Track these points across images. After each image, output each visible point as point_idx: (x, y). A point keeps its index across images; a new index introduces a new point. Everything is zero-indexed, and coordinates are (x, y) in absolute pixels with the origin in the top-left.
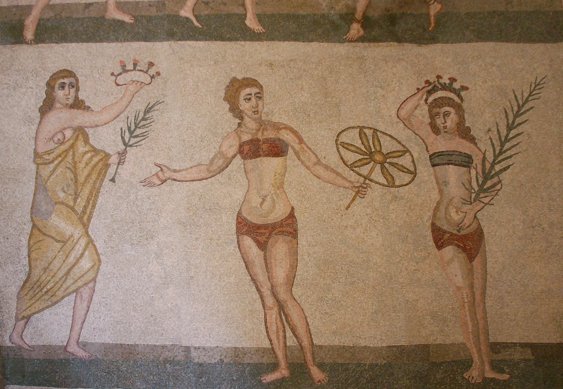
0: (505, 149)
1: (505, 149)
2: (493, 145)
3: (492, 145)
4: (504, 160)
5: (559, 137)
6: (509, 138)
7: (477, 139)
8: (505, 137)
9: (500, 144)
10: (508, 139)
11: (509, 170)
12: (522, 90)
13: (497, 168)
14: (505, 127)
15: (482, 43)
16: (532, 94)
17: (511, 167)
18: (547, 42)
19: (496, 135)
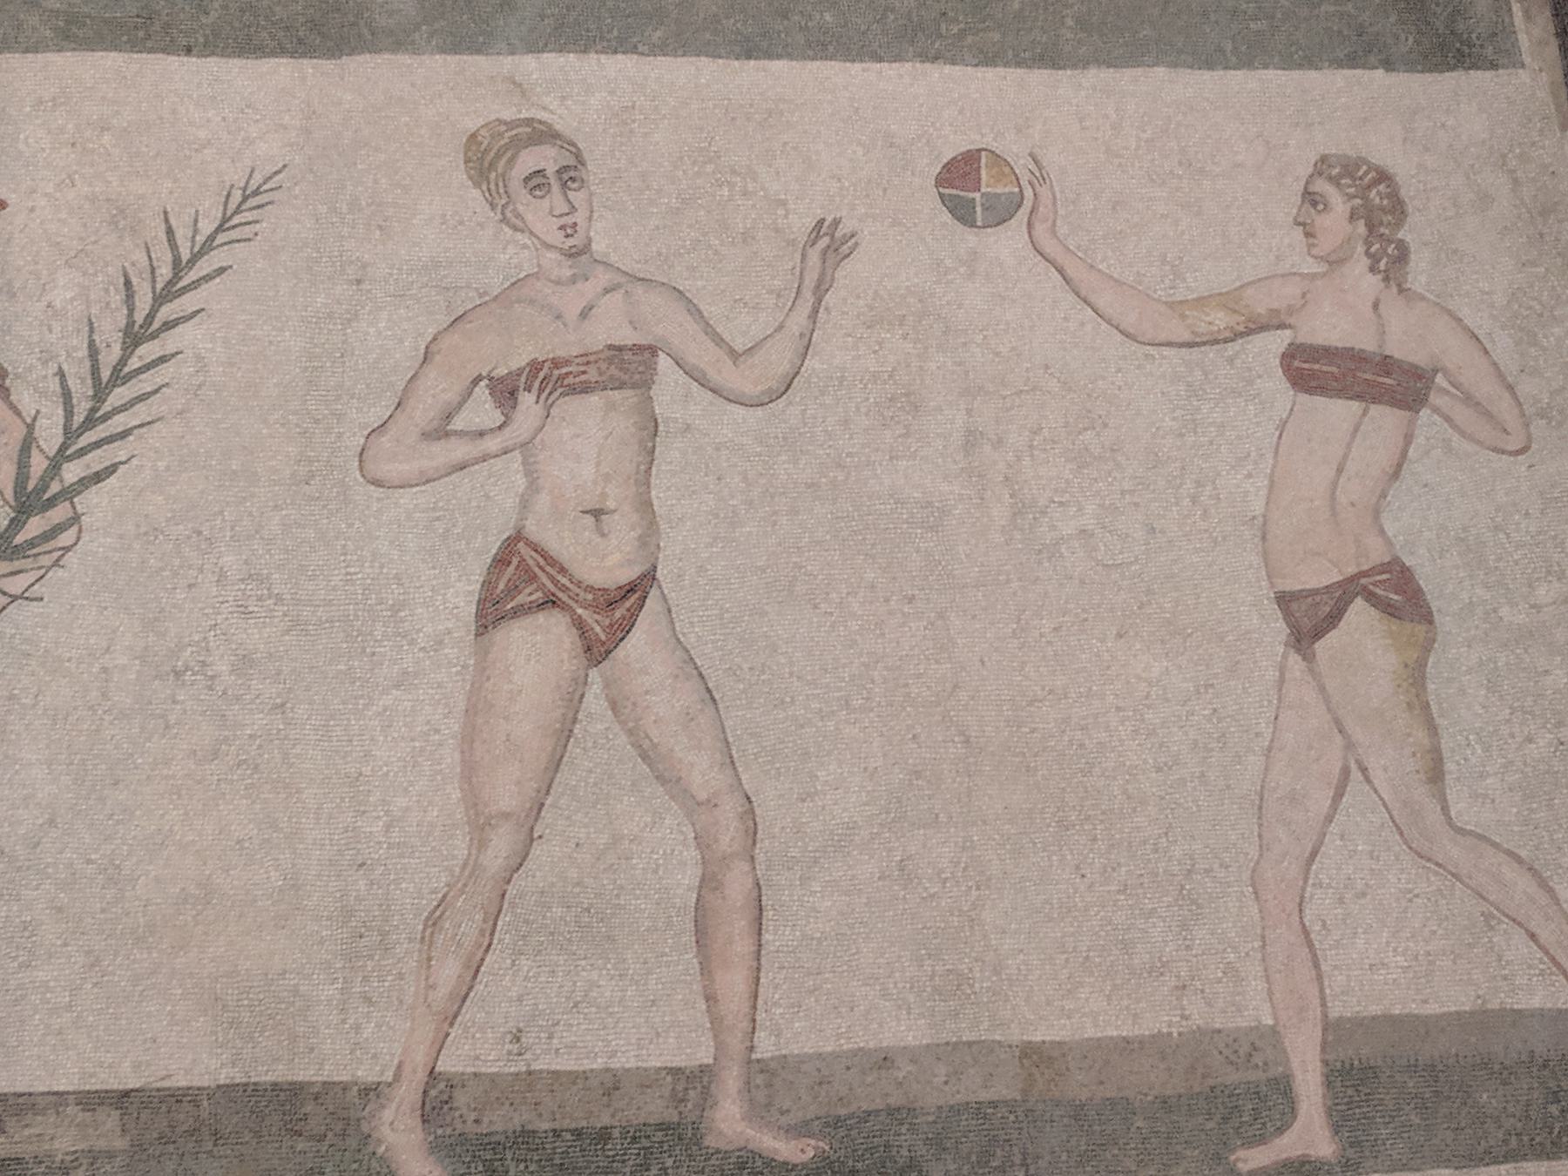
0: (110, 409)
1: (107, 407)
2: (67, 395)
3: (64, 394)
4: (97, 445)
5: (306, 368)
6: (126, 370)
7: (11, 376)
8: (115, 367)
9: (91, 393)
10: (122, 374)
11: (112, 480)
12: (197, 211)
13: (72, 472)
14: (120, 334)
15: (77, 53)
16: (227, 226)
17: (122, 469)
18: (303, 55)
19: (81, 361)
